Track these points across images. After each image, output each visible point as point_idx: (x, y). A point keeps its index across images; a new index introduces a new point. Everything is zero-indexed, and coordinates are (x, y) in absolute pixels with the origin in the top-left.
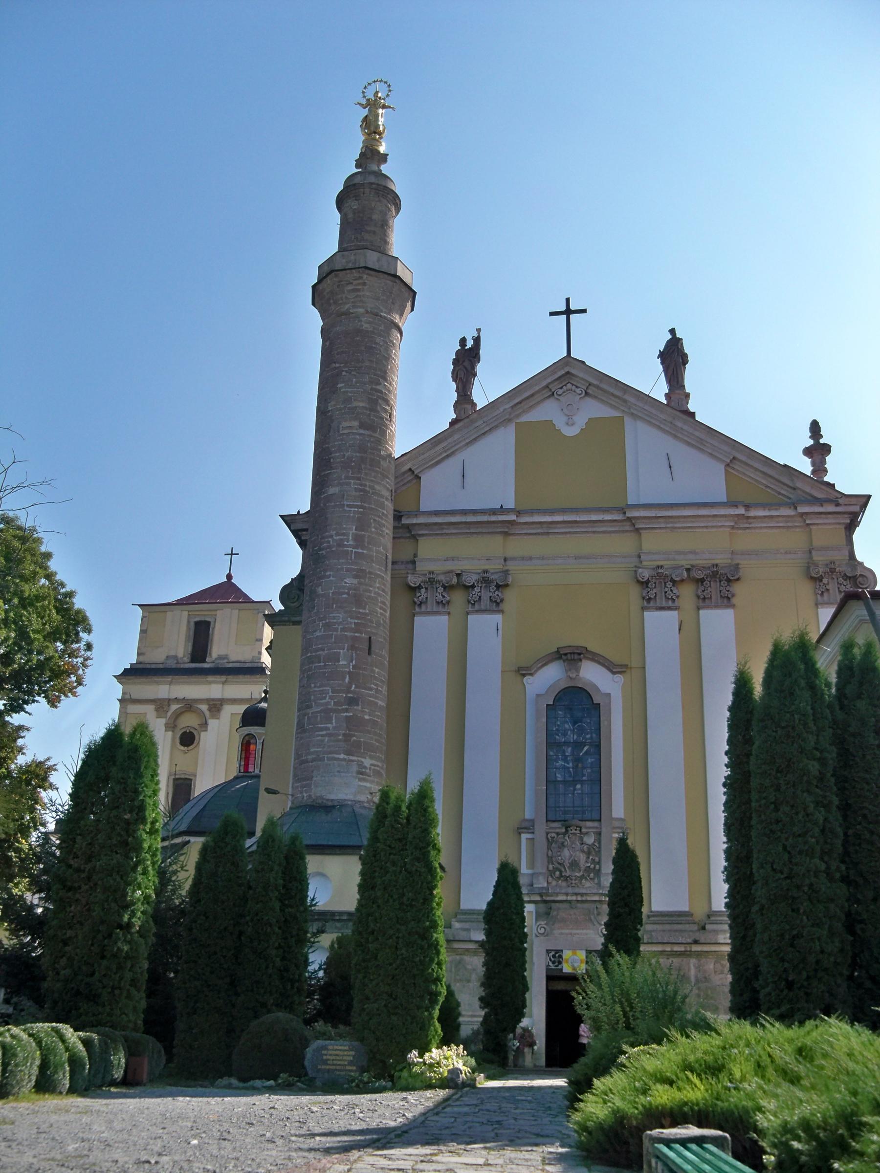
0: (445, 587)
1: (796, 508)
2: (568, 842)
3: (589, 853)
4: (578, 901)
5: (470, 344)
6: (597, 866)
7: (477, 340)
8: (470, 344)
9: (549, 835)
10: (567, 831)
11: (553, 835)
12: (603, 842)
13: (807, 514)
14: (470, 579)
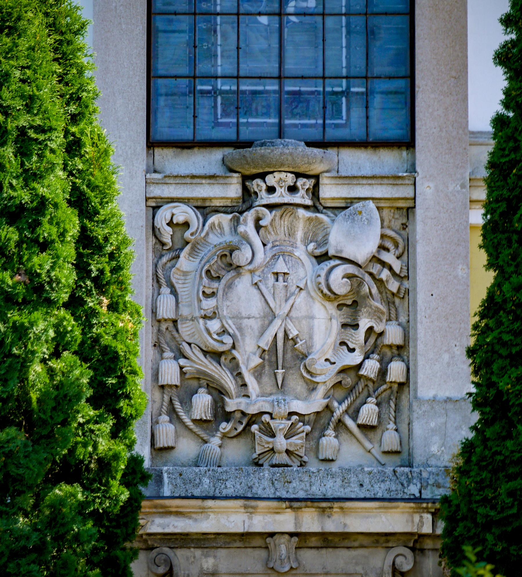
2: (254, 252)
3: (351, 306)
4: (301, 538)
6: (396, 370)
9: (163, 216)
10: (248, 196)
11: (183, 213)
12: (422, 251)
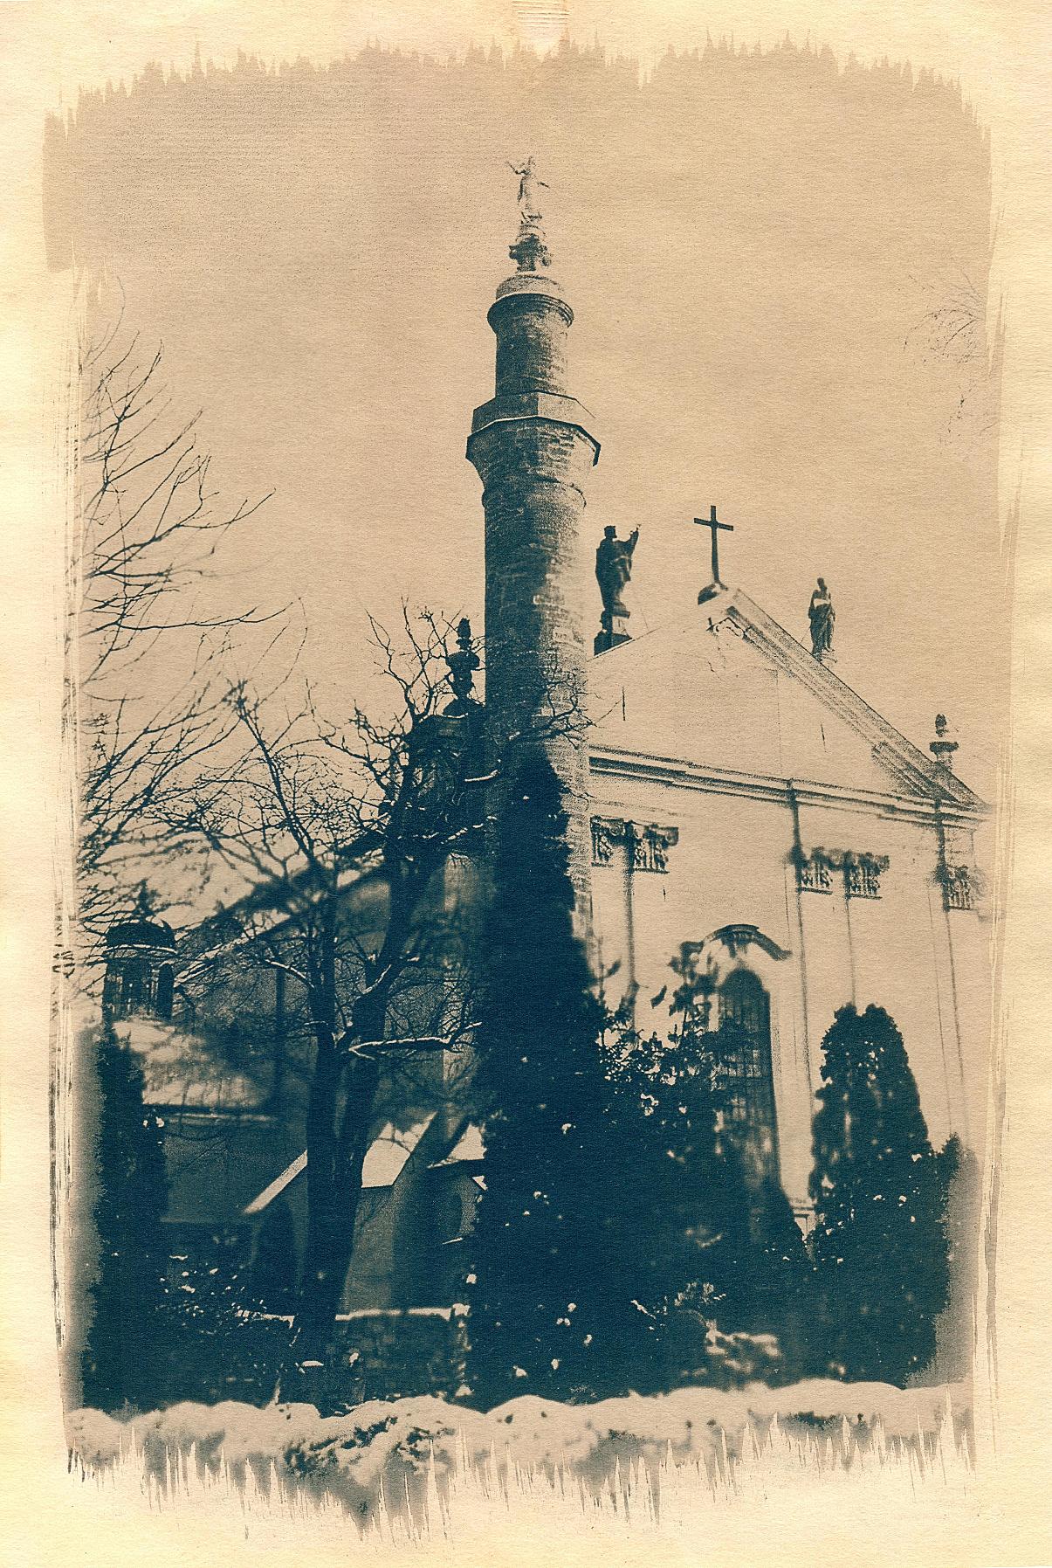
0: (608, 835)
1: (936, 806)
5: (622, 536)
7: (635, 535)
8: (622, 536)
13: (950, 816)
14: (640, 832)
